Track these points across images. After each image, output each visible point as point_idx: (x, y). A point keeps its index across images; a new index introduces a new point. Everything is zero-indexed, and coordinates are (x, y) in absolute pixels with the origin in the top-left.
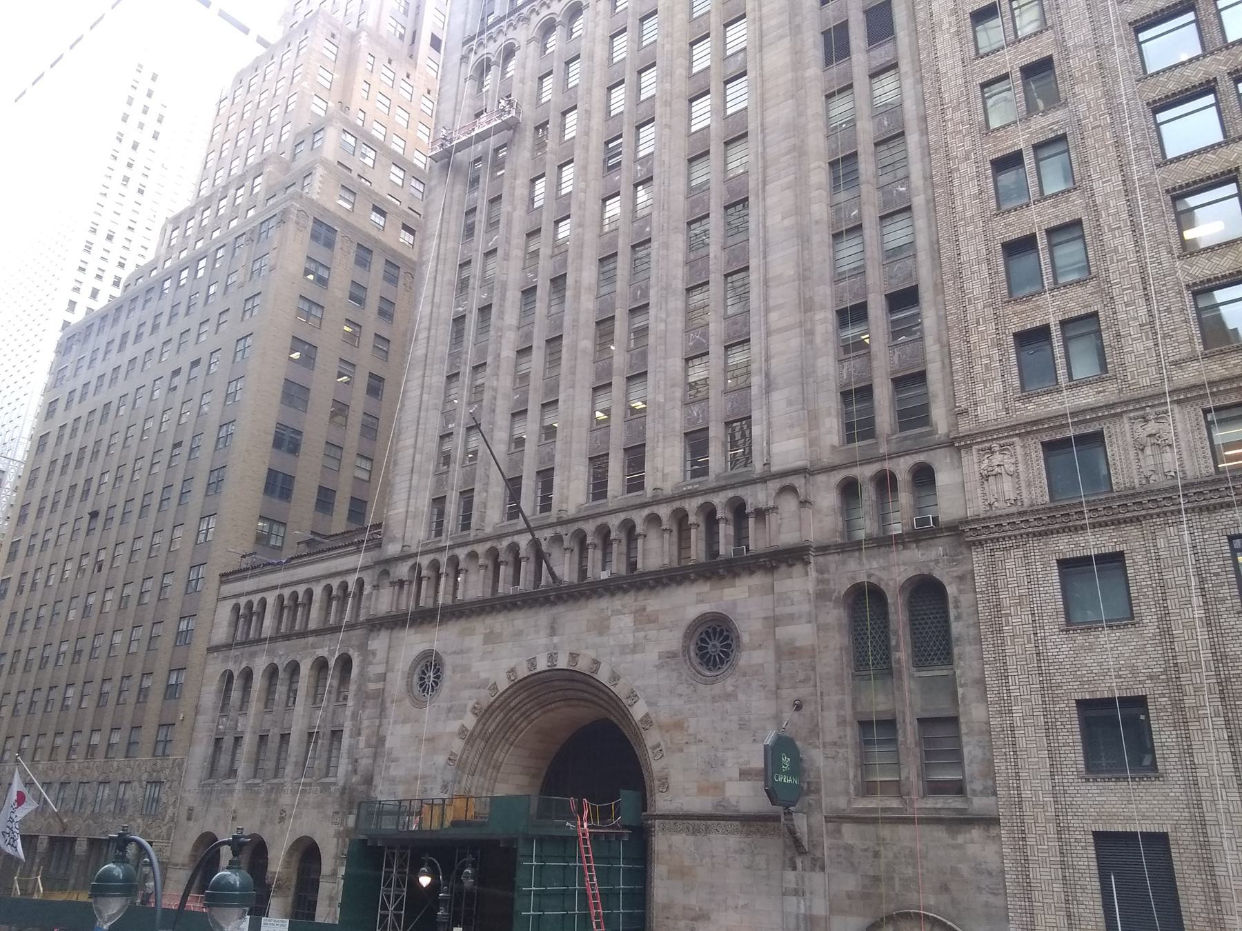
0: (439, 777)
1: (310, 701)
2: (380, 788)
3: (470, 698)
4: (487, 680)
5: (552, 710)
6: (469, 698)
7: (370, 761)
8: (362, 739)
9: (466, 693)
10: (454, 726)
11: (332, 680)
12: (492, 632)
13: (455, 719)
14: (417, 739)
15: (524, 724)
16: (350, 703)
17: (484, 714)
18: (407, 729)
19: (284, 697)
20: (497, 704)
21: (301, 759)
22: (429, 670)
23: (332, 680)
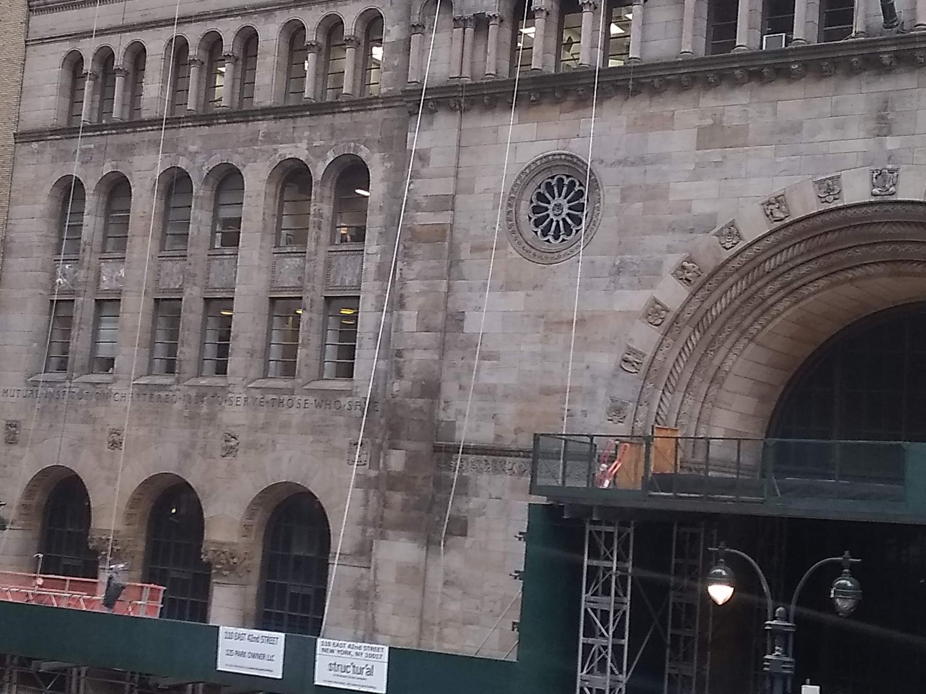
0: (602, 394)
1: (270, 240)
2: (456, 405)
3: (670, 250)
4: (712, 218)
5: (851, 280)
6: (666, 250)
7: (431, 355)
8: (410, 320)
9: (661, 240)
10: (637, 300)
11: (321, 205)
12: (717, 125)
13: (631, 287)
14: (553, 324)
15: (786, 303)
16: (372, 246)
17: (702, 281)
18: (516, 301)
19: (206, 231)
20: (735, 264)
21: (260, 345)
22: (559, 199)
23: (321, 205)
